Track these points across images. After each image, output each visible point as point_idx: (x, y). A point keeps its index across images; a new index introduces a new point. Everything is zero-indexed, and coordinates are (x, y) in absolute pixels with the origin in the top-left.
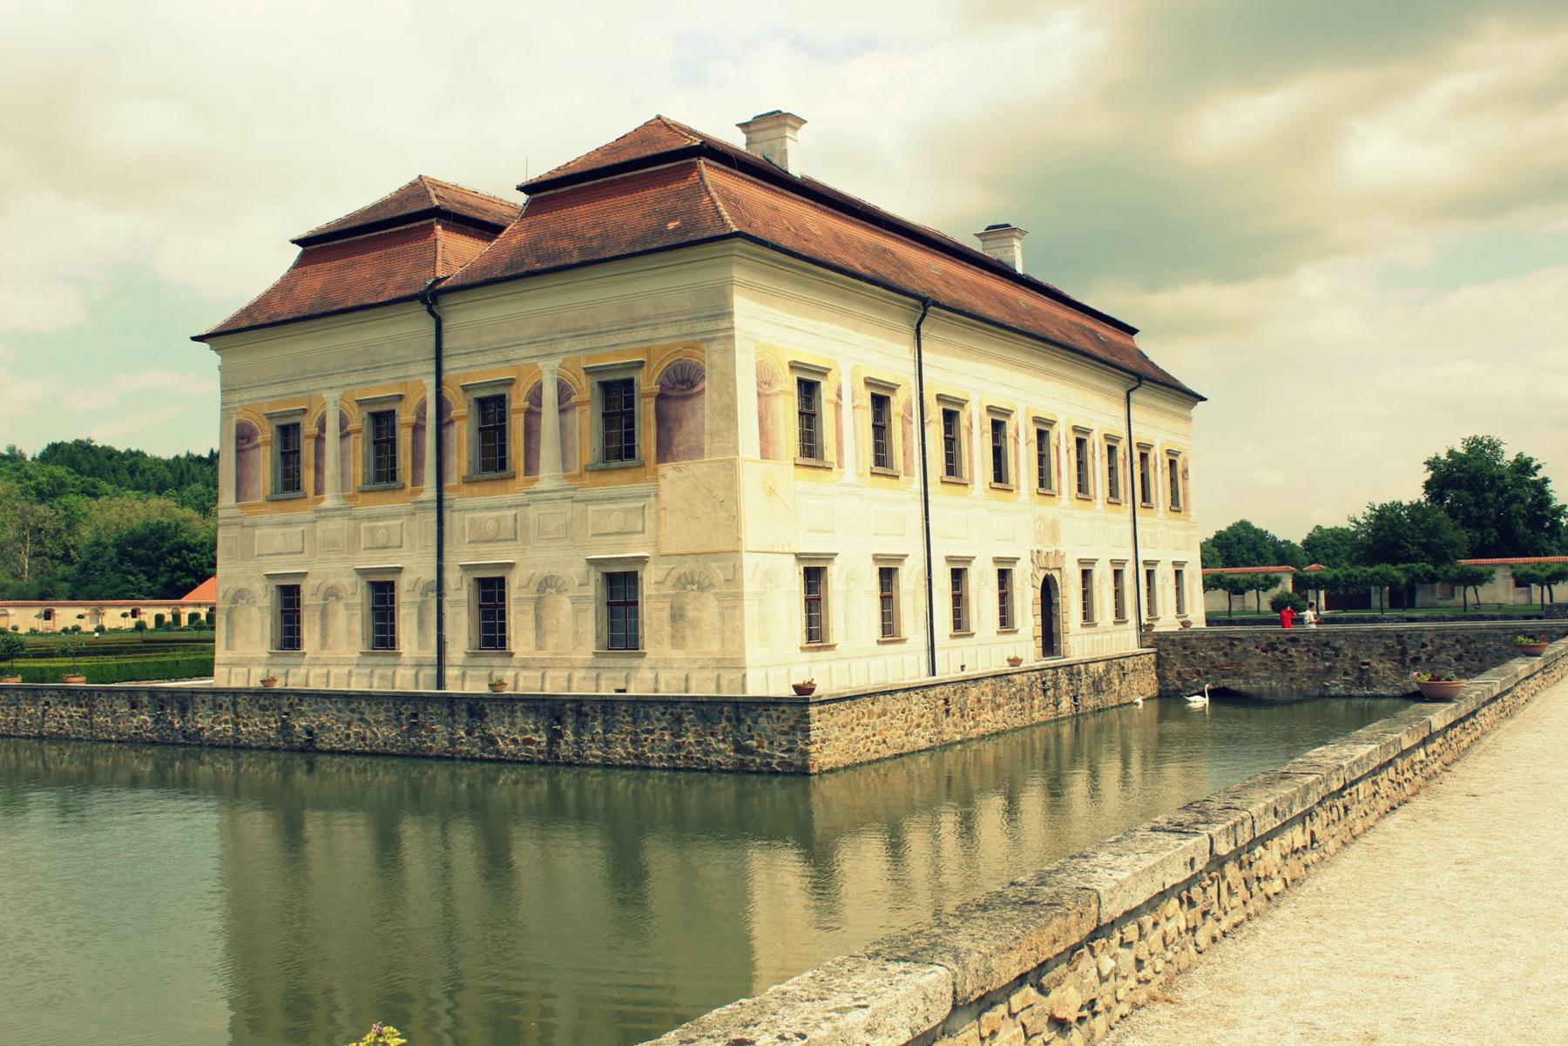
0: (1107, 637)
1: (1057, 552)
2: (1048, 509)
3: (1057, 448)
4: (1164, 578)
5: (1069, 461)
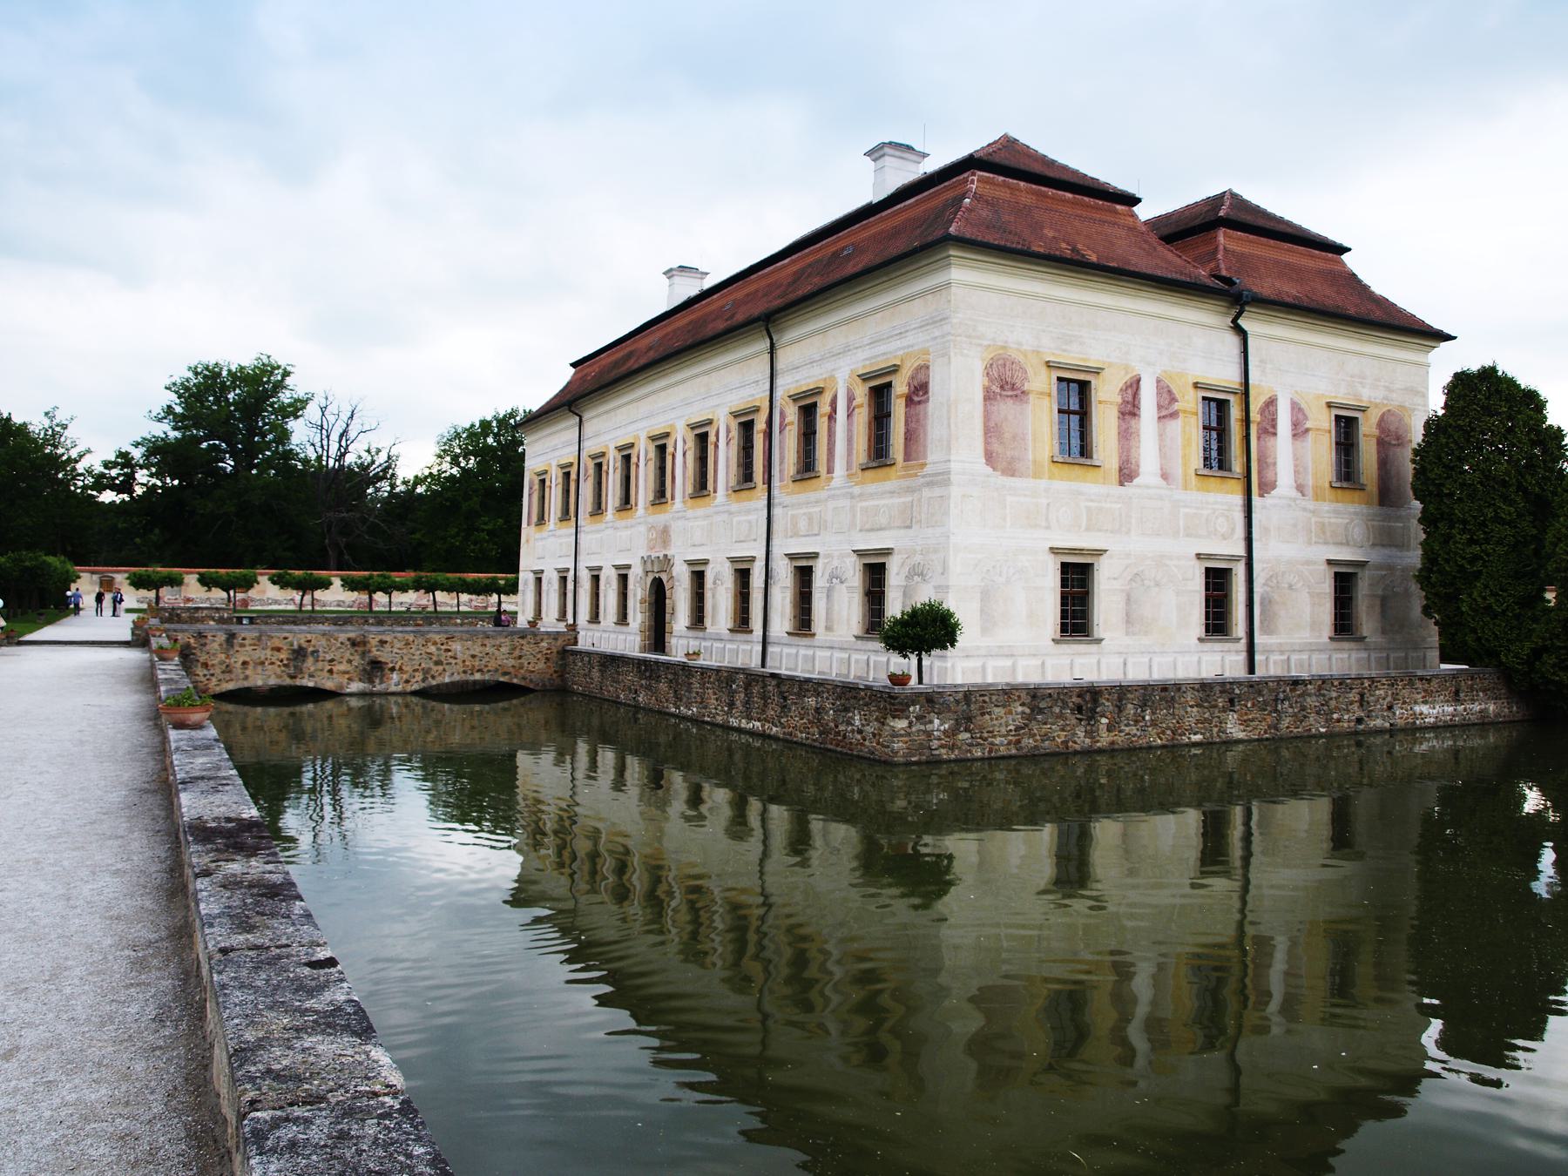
0: (605, 635)
1: (666, 556)
2: (661, 517)
4: (549, 583)
5: (685, 462)
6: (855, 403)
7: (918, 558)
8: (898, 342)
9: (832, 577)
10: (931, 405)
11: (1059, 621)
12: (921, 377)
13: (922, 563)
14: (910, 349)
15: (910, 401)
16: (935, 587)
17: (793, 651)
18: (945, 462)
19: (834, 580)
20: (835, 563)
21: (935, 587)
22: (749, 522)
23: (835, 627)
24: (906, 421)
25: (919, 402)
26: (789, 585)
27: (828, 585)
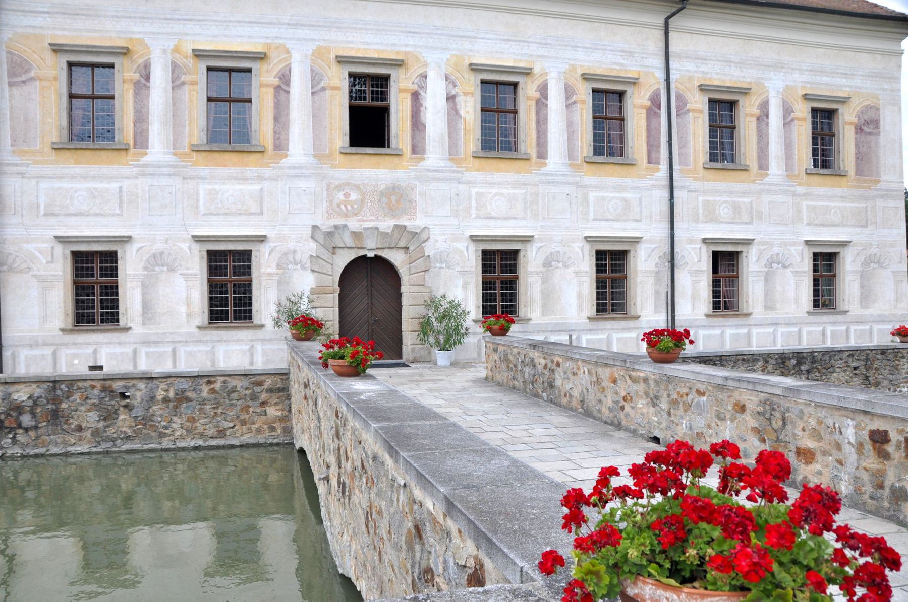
1: (402, 228)
3: (416, 96)
6: (792, 115)
7: (874, 250)
8: (844, 80)
9: (770, 263)
10: (882, 138)
11: (812, 298)
12: (871, 114)
13: (878, 254)
14: (858, 90)
15: (859, 130)
16: (893, 272)
17: (717, 332)
18: (900, 183)
19: (775, 265)
20: (776, 250)
21: (893, 272)
22: (625, 200)
23: (778, 306)
24: (857, 146)
25: (870, 133)
26: (705, 269)
27: (766, 269)
